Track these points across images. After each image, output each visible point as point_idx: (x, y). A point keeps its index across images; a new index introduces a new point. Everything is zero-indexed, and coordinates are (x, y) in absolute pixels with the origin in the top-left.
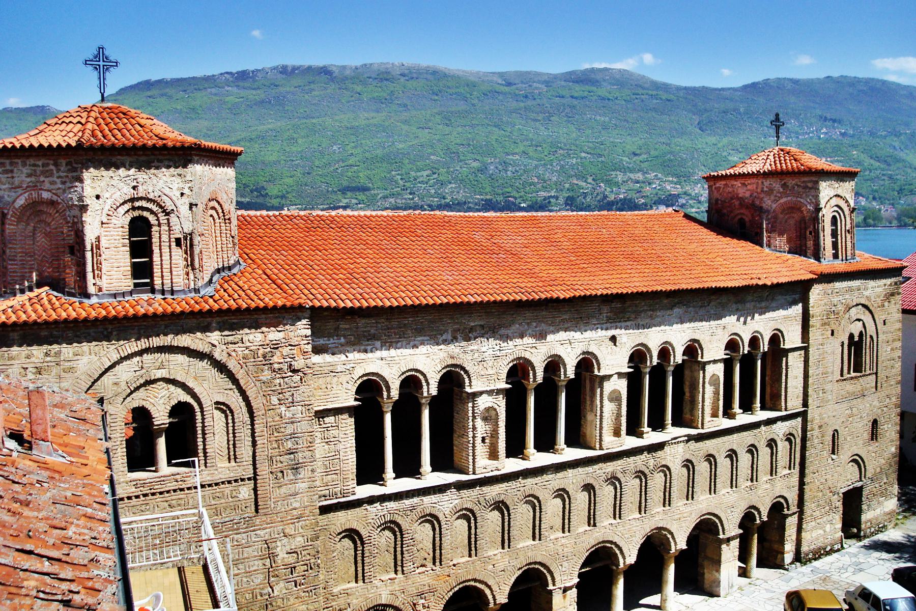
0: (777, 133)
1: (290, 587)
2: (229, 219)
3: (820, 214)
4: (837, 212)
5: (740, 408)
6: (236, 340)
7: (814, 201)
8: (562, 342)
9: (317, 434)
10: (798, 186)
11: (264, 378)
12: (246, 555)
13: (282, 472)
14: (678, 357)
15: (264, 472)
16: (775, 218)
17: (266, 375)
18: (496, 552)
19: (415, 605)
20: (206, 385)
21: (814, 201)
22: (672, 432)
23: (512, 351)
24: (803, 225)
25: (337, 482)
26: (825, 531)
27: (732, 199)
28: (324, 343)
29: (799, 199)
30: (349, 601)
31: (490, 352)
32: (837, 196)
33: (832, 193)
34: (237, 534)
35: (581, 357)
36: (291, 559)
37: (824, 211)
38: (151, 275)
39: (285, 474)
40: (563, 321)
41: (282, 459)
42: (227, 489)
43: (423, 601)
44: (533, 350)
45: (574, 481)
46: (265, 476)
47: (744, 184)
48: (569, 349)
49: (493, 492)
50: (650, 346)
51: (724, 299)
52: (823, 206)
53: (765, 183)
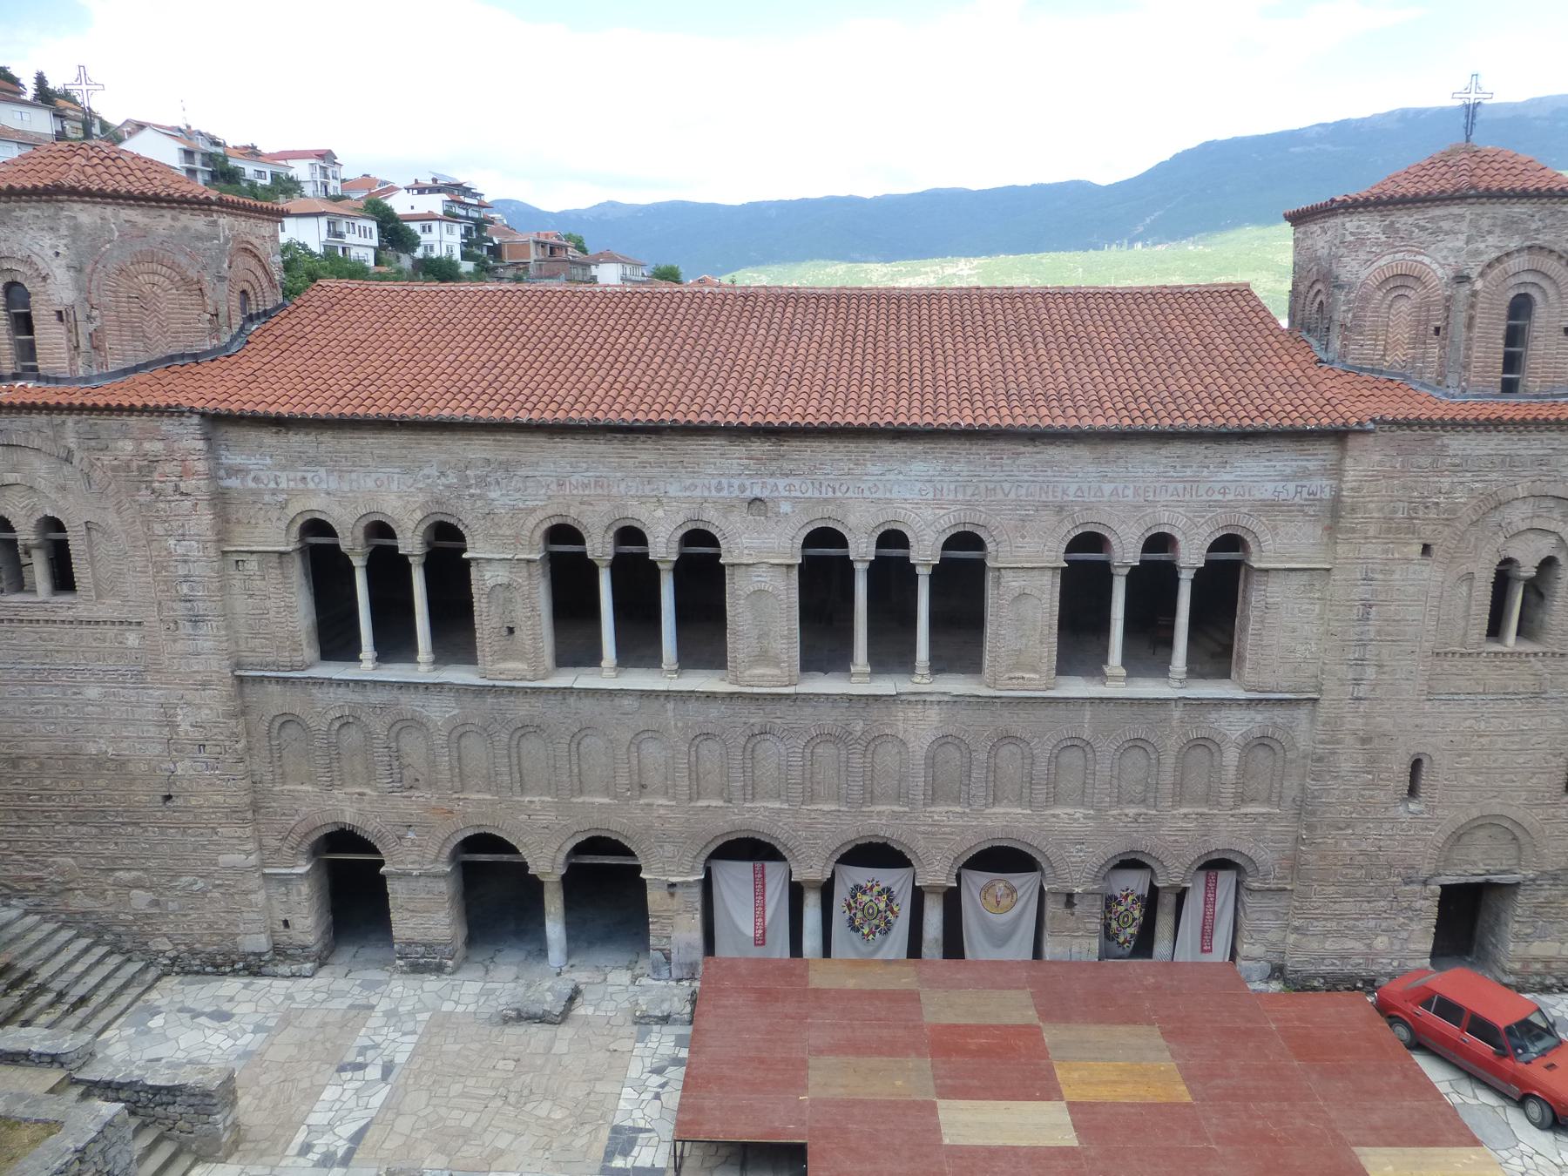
1: (200, 769)
2: (200, 289)
3: (1465, 289)
5: (1124, 664)
6: (100, 446)
7: (1451, 260)
8: (643, 500)
9: (234, 582)
10: (1423, 229)
11: (142, 499)
12: (137, 717)
13: (176, 623)
14: (925, 553)
15: (152, 619)
16: (1366, 299)
17: (144, 496)
18: (534, 799)
19: (400, 838)
20: (70, 497)
21: (1451, 260)
22: (921, 681)
23: (543, 503)
25: (268, 650)
26: (1369, 946)
28: (242, 462)
29: (1419, 258)
30: (296, 806)
34: (122, 688)
35: (690, 526)
36: (197, 734)
37: (1479, 285)
38: (32, 356)
39: (181, 626)
40: (643, 464)
41: (175, 605)
42: (111, 631)
43: (411, 835)
44: (584, 507)
45: (680, 724)
46: (154, 624)
48: (660, 513)
49: (522, 709)
50: (852, 520)
53: (1348, 225)
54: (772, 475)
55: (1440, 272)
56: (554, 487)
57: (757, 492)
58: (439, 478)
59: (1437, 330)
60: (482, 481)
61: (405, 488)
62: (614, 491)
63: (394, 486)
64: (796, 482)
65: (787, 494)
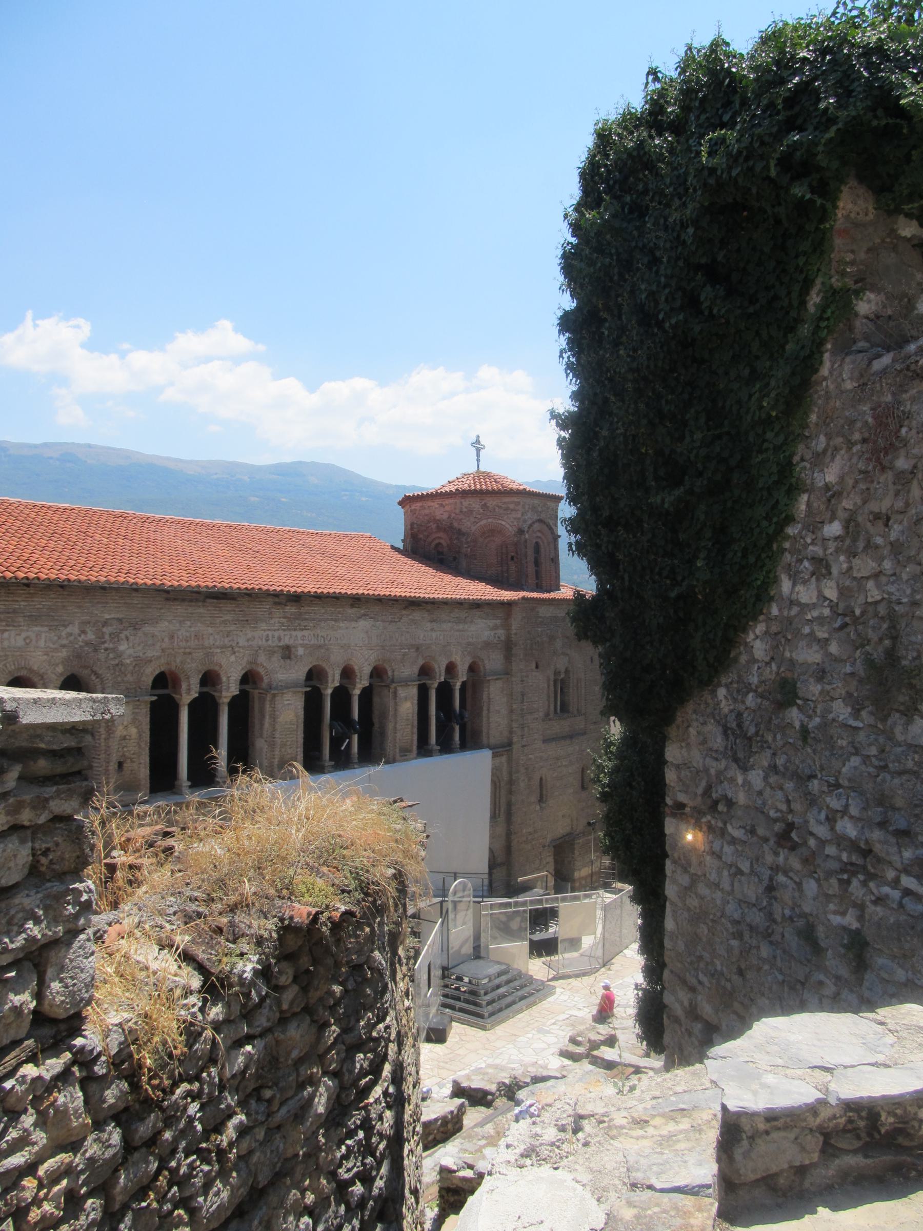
0: (478, 455)
3: (523, 537)
4: (538, 537)
24: (504, 551)
27: (429, 522)
31: (131, 651)
32: (540, 521)
33: (535, 517)
35: (248, 667)
37: (527, 536)
40: (225, 622)
47: (441, 505)
48: (233, 658)
51: (417, 615)
52: (526, 529)
54: (295, 630)
55: (510, 529)
56: (166, 640)
57: (286, 641)
58: (80, 636)
59: (512, 558)
60: (115, 636)
61: (52, 646)
62: (206, 643)
63: (42, 643)
64: (306, 633)
65: (301, 642)
